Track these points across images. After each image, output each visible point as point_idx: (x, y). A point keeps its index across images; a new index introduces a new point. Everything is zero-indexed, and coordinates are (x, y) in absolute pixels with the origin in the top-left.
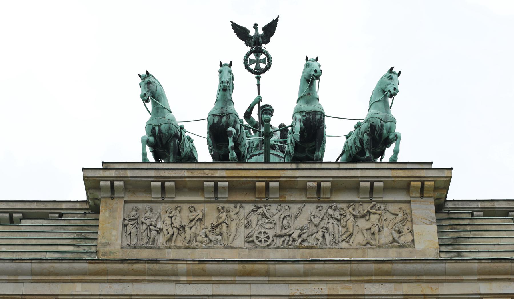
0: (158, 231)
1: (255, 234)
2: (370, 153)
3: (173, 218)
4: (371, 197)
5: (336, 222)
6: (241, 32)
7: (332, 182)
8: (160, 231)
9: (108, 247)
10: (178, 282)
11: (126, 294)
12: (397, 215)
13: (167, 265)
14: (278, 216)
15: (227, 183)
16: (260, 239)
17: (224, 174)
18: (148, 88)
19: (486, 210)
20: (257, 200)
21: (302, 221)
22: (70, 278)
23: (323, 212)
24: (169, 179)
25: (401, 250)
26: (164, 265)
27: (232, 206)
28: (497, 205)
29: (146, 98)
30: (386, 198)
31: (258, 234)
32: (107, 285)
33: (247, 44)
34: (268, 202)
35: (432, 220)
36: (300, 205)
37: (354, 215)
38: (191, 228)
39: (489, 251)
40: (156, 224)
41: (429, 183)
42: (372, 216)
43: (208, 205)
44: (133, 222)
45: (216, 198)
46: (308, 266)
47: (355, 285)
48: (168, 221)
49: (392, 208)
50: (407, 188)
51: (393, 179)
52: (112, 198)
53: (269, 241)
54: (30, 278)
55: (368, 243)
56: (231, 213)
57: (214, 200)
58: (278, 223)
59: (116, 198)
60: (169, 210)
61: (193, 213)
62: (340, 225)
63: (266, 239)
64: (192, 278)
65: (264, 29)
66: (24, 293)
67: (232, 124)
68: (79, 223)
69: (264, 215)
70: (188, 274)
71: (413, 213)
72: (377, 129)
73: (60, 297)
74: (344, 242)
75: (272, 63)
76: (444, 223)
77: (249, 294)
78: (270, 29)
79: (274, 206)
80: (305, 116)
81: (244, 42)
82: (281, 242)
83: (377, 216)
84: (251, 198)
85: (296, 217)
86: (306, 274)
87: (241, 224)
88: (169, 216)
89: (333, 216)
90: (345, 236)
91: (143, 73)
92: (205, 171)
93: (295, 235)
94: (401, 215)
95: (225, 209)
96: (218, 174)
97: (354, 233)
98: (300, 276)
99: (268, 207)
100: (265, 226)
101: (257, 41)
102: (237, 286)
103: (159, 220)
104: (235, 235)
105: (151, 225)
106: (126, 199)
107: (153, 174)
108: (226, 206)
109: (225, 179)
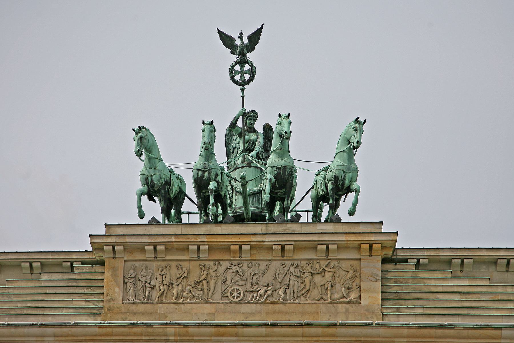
1: (230, 290)
2: (333, 200)
3: (164, 276)
5: (297, 279)
6: (226, 40)
8: (153, 288)
9: (112, 302)
14: (249, 273)
15: (207, 247)
16: (233, 295)
17: (204, 239)
18: (141, 142)
21: (268, 278)
23: (286, 269)
24: (160, 244)
26: (156, 329)
27: (211, 263)
29: (139, 154)
31: (232, 290)
33: (233, 53)
34: (241, 260)
36: (267, 263)
38: (178, 285)
40: (150, 282)
42: (326, 273)
45: (199, 257)
48: (160, 279)
49: (345, 265)
52: (114, 258)
53: (241, 297)
55: (322, 298)
56: (211, 271)
57: (197, 259)
58: (248, 279)
62: (299, 281)
63: (238, 295)
67: (214, 178)
74: (302, 298)
76: (390, 275)
79: (246, 264)
80: (275, 171)
81: (230, 50)
82: (250, 297)
84: (227, 257)
85: (264, 274)
86: (267, 336)
87: (218, 280)
88: (160, 275)
89: (294, 274)
90: (304, 291)
91: (136, 128)
92: (189, 236)
93: (262, 292)
94: (351, 272)
95: (206, 266)
97: (311, 289)
98: (263, 336)
99: (241, 265)
100: (238, 283)
103: (153, 277)
105: (146, 282)
106: (125, 259)
107: (146, 240)
108: (207, 263)
109: (206, 243)
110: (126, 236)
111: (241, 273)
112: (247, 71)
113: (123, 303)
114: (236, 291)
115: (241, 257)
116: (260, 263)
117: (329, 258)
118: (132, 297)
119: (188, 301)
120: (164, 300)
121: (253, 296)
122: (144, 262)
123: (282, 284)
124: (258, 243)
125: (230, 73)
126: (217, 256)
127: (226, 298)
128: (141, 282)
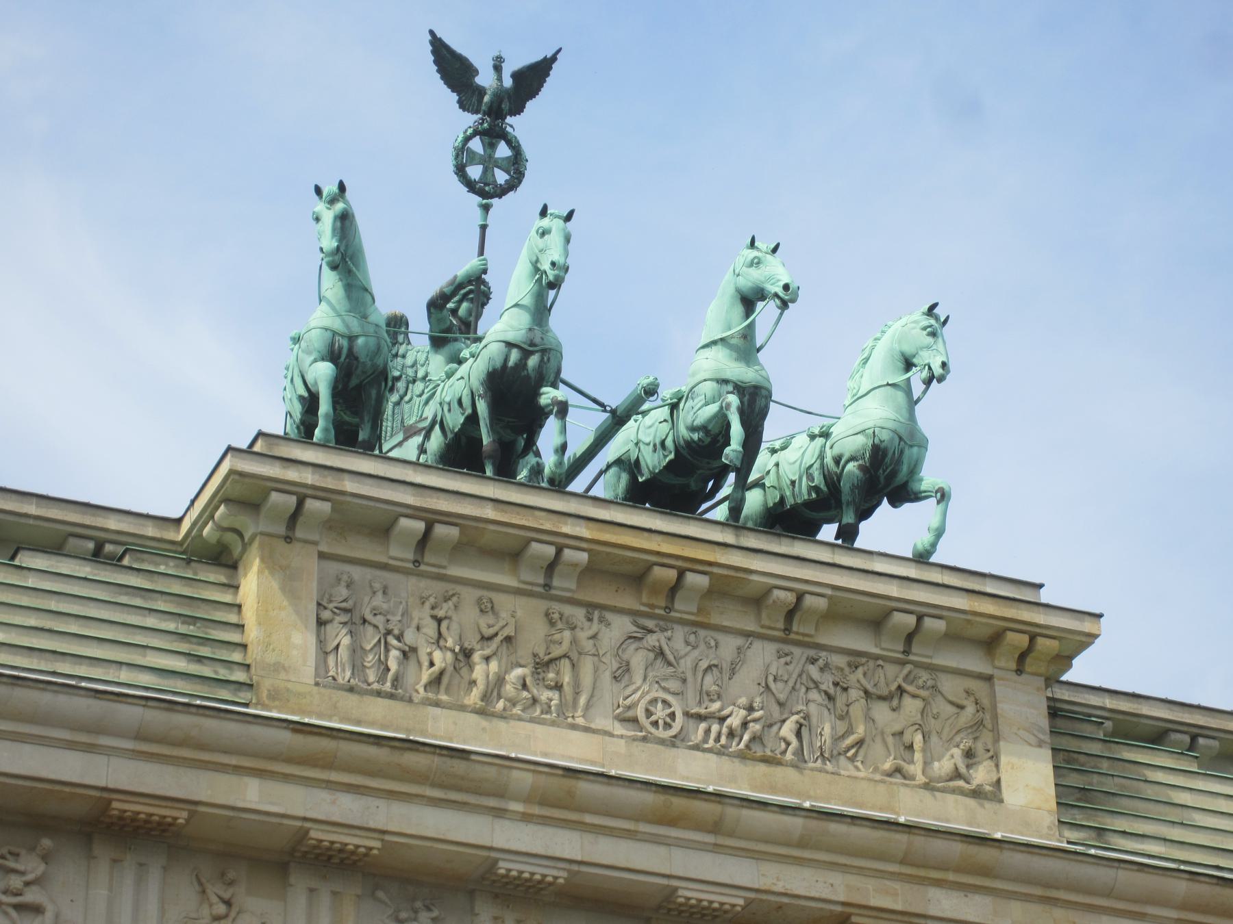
0: (404, 653)
3: (444, 624)
4: (906, 652)
5: (826, 702)
6: (453, 68)
7: (830, 598)
9: (283, 675)
10: (499, 813)
11: (372, 825)
12: (962, 707)
13: (487, 768)
16: (653, 718)
19: (1121, 717)
20: (643, 608)
22: (233, 760)
23: (795, 669)
25: (971, 803)
26: (478, 767)
27: (579, 614)
28: (1145, 709)
30: (939, 660)
32: (323, 795)
33: (463, 105)
34: (667, 621)
35: (1042, 737)
36: (739, 641)
37: (866, 692)
38: (487, 659)
39: (1165, 840)
41: (1048, 642)
42: (907, 701)
43: (522, 601)
44: (344, 618)
45: (547, 586)
46: (814, 824)
47: (907, 886)
48: (430, 629)
49: (950, 686)
50: (991, 643)
51: (969, 617)
52: (288, 539)
54: (129, 745)
56: (582, 635)
57: (540, 590)
58: (690, 679)
59: (299, 540)
60: (432, 600)
61: (490, 619)
63: (668, 720)
64: (536, 810)
65: (516, 76)
66: (111, 786)
68: (177, 588)
69: (661, 653)
70: (528, 800)
71: (999, 711)
72: (888, 460)
73: (201, 809)
74: (842, 758)
75: (526, 173)
77: (668, 872)
78: (532, 79)
79: (679, 633)
81: (455, 97)
83: (918, 704)
85: (733, 672)
86: (802, 844)
88: (434, 617)
89: (823, 687)
92: (537, 513)
94: (970, 709)
96: (568, 528)
97: (868, 740)
98: (788, 844)
101: (494, 104)
102: (638, 845)
104: (592, 696)
105: (389, 632)
106: (324, 548)
108: (568, 610)
109: (584, 545)
110: (346, 476)
111: (671, 658)
112: (503, 159)
113: (317, 684)
114: (660, 705)
115: (669, 608)
116: (721, 637)
117: (911, 657)
118: (344, 670)
119: (517, 710)
120: (444, 697)
121: (708, 732)
122: (378, 573)
123: (787, 711)
124: (732, 573)
125: (457, 156)
126: (602, 595)
127: (630, 725)
128: (370, 629)
